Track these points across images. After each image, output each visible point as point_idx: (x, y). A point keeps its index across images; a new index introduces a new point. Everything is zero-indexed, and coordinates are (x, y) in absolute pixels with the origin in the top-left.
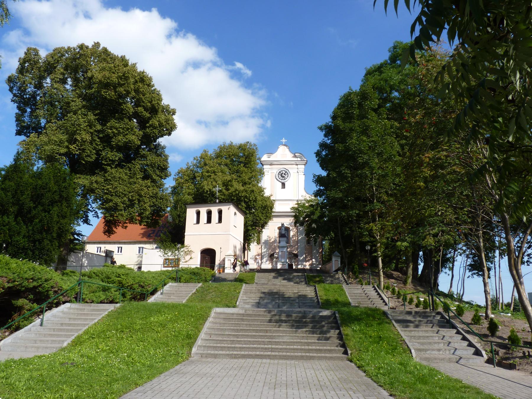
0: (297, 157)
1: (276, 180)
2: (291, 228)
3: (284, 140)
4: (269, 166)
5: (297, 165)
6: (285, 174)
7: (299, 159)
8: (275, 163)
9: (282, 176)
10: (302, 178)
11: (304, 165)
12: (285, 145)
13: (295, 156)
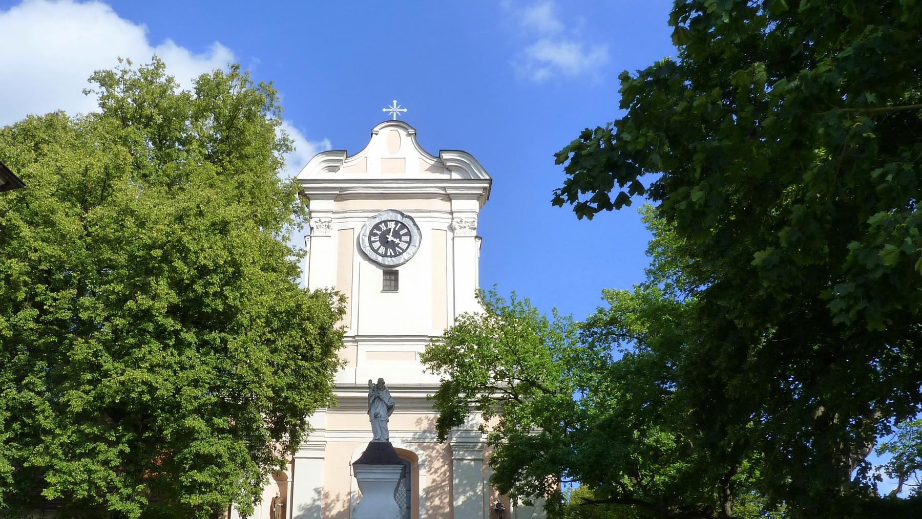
0: (449, 170)
1: (358, 258)
2: (422, 455)
3: (395, 110)
4: (330, 205)
5: (448, 198)
6: (396, 234)
7: (455, 176)
8: (360, 189)
9: (385, 243)
10: (469, 250)
11: (478, 197)
12: (400, 123)
13: (442, 166)
